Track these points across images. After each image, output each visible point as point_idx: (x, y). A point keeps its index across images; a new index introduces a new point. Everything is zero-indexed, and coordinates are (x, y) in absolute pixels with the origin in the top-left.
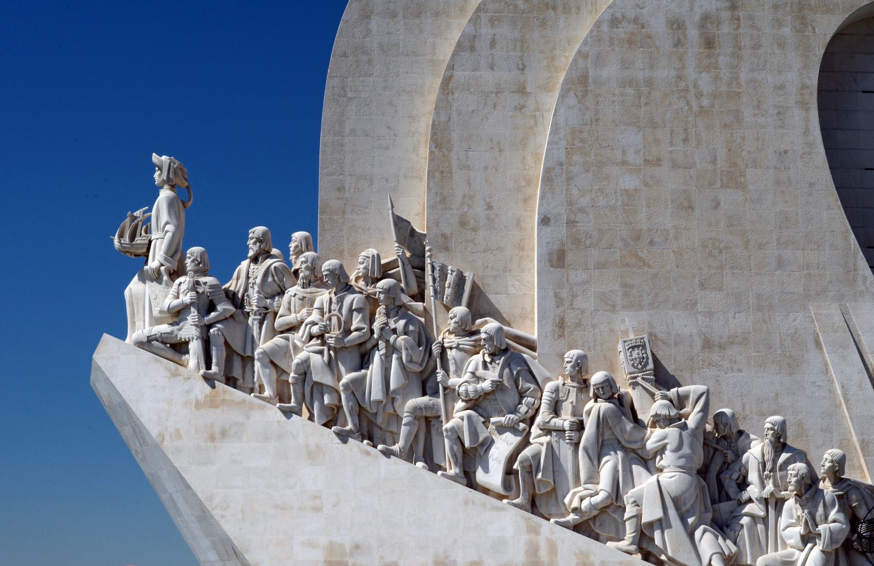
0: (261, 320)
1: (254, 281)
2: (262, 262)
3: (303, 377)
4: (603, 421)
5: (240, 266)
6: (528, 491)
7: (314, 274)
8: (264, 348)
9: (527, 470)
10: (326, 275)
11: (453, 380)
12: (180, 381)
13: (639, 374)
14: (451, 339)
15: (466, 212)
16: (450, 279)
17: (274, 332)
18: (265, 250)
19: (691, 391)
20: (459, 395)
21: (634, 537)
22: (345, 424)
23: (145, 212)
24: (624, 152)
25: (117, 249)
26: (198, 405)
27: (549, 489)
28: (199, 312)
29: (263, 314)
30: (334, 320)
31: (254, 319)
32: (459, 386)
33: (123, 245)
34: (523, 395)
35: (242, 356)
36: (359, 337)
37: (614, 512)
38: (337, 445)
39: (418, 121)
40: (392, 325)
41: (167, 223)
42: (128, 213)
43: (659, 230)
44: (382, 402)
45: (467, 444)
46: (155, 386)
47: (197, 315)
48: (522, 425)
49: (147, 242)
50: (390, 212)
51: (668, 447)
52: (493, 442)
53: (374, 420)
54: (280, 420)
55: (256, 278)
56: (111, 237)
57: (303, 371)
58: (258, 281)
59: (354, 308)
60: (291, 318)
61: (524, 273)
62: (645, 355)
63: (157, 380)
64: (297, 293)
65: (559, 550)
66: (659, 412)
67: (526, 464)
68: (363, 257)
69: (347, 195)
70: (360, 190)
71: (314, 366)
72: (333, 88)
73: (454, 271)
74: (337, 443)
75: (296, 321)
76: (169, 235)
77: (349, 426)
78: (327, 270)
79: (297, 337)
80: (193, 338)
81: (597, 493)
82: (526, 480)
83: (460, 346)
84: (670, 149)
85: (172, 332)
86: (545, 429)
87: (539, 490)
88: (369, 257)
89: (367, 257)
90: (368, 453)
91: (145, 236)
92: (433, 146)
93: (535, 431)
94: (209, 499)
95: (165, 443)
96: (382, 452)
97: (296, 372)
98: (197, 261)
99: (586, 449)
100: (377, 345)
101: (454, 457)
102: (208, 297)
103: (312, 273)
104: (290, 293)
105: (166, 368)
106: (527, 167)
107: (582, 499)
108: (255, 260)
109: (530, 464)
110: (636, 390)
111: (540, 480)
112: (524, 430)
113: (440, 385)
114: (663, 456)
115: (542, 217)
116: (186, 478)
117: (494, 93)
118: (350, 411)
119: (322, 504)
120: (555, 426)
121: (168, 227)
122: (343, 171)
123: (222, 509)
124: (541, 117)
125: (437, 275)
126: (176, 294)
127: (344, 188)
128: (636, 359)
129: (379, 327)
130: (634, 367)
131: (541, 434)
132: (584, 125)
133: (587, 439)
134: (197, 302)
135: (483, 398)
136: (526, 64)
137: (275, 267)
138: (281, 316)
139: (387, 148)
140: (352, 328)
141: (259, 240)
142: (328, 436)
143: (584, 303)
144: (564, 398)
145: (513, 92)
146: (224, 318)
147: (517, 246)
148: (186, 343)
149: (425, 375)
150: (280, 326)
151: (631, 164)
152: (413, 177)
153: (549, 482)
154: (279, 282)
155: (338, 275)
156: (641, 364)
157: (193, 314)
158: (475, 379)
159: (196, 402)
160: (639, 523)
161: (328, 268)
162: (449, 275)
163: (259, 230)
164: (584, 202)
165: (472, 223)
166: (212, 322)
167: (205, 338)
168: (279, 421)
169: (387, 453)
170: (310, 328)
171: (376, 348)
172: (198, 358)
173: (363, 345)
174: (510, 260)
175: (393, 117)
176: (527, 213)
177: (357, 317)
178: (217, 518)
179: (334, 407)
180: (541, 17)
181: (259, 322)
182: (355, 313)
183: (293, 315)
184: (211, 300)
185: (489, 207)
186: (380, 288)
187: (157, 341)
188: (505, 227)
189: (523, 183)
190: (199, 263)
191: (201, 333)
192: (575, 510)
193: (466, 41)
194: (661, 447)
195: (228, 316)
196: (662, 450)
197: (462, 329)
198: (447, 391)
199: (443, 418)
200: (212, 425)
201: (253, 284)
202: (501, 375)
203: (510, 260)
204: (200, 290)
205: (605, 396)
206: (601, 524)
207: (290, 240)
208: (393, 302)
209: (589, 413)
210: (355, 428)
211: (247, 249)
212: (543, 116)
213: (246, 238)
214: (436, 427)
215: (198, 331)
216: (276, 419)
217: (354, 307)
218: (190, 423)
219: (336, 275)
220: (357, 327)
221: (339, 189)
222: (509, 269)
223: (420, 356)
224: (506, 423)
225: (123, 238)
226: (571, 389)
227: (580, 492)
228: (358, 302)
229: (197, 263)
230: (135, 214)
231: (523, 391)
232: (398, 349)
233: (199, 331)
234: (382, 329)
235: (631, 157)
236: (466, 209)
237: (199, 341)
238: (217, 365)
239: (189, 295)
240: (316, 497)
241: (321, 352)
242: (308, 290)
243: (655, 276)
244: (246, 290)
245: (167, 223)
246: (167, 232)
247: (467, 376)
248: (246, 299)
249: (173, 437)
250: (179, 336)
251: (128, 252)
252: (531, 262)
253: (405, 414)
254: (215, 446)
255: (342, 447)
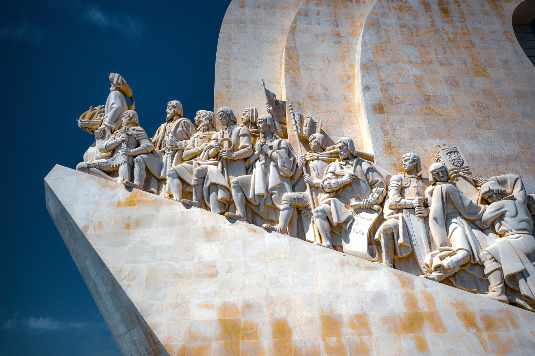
0: (173, 155)
1: (169, 131)
2: (175, 121)
3: (202, 180)
4: (446, 198)
5: (161, 127)
6: (391, 256)
7: (211, 124)
8: (175, 168)
9: (389, 237)
10: (220, 116)
11: (316, 181)
12: (108, 190)
13: (461, 170)
14: (312, 154)
15: (312, 91)
16: (306, 122)
17: (183, 161)
18: (178, 114)
19: (507, 177)
20: (323, 188)
21: (502, 287)
22: (235, 210)
23: (101, 108)
24: (409, 57)
25: (80, 127)
26: (119, 204)
27: (409, 254)
28: (128, 146)
29: (174, 151)
30: (226, 144)
31: (167, 154)
32: (323, 182)
33: (83, 122)
34: (373, 186)
35: (158, 179)
36: (245, 152)
37: (471, 269)
38: (229, 227)
39: (275, 55)
40: (269, 144)
41: (113, 104)
42: (90, 107)
43: (441, 96)
44: (263, 196)
45: (335, 220)
46: (88, 194)
47: (126, 147)
48: (376, 207)
49: (100, 121)
50: (263, 86)
51: (507, 214)
52: (354, 220)
53: (257, 212)
54: (183, 211)
55: (170, 130)
56: (77, 120)
57: (202, 176)
58: (172, 129)
59: (240, 134)
60: (194, 150)
61: (353, 125)
62: (460, 158)
63: (90, 190)
64: (199, 135)
65: (436, 301)
66: (492, 188)
67: (389, 232)
68: (246, 111)
69: (232, 90)
70: (241, 87)
71: (211, 172)
72: (224, 37)
73: (309, 118)
74: (228, 225)
75: (198, 151)
76: (114, 109)
77: (238, 213)
78: (221, 111)
79: (199, 160)
80: (122, 164)
81: (454, 253)
82: (389, 246)
83: (319, 157)
84: (436, 56)
85: (107, 163)
86: (395, 209)
87: (401, 255)
88: (250, 110)
89: (248, 110)
90: (255, 231)
91: (99, 118)
92: (287, 59)
93: (387, 211)
94: (119, 273)
95: (89, 232)
96: (265, 228)
97: (197, 176)
98: (130, 117)
99: (435, 219)
100: (259, 158)
101: (325, 232)
102: (136, 138)
103: (209, 122)
104: (194, 136)
105: (98, 182)
106: (346, 71)
107: (442, 258)
108: (171, 120)
109: (392, 232)
110: (459, 181)
111: (401, 245)
112: (379, 210)
113: (307, 184)
114: (502, 222)
115: (365, 87)
116: (101, 258)
117: (322, 35)
118: (239, 202)
119: (217, 271)
120: (405, 204)
121: (114, 106)
122: (229, 78)
123: (129, 280)
124: (351, 48)
125: (297, 119)
126: (113, 139)
127: (230, 86)
128: (455, 160)
129: (259, 144)
130: (455, 165)
131: (393, 212)
132: (382, 43)
133: (435, 212)
134: (127, 140)
135: (342, 191)
136: (338, 23)
137: (184, 122)
138: (187, 149)
139: (257, 67)
140: (239, 147)
141: (173, 107)
142: (222, 220)
143: (402, 134)
144: (408, 185)
145: (333, 35)
146: (147, 152)
147: (346, 110)
148: (118, 167)
149: (294, 181)
150: (187, 155)
151: (414, 62)
152: (273, 82)
153: (409, 247)
154: (187, 131)
155: (229, 115)
156: (460, 164)
157: (123, 147)
158: (334, 176)
159: (118, 202)
160: (503, 276)
161: (222, 110)
162: (305, 120)
163: (174, 102)
164: (390, 80)
165: (316, 97)
166: (137, 153)
167: (131, 164)
168: (182, 212)
169: (269, 230)
170: (208, 152)
171: (258, 161)
172: (124, 176)
173: (247, 160)
174: (343, 118)
175: (260, 53)
176: (350, 94)
177: (243, 140)
178: (124, 288)
179: (226, 203)
180: (344, 4)
181: (172, 156)
182: (241, 138)
183: (196, 148)
184: (137, 140)
185: (326, 89)
186: (259, 120)
187: (96, 168)
188: (337, 100)
189: (345, 78)
190: (131, 119)
191: (128, 159)
192: (439, 268)
193: (303, 12)
194: (499, 215)
195: (149, 151)
196: (501, 217)
197: (320, 147)
198: (313, 189)
199: (312, 206)
200: (129, 217)
201: (169, 133)
202: (354, 171)
203: (343, 118)
204: (130, 133)
205: (444, 179)
206: (461, 280)
207: (195, 115)
208: (269, 129)
209: (431, 193)
210: (243, 214)
211: (166, 114)
212: (352, 47)
213: (166, 107)
214: (306, 214)
215: (125, 158)
216: (180, 211)
217: (240, 134)
218: (111, 217)
219: (228, 114)
220: (243, 145)
221: (227, 87)
222: (343, 123)
223: (291, 164)
224: (364, 205)
225: (84, 118)
226: (412, 179)
227: (437, 254)
228: (243, 131)
229: (129, 118)
230: (95, 108)
231: (372, 184)
232: (274, 160)
233: (127, 157)
234: (262, 146)
235: (413, 59)
236: (311, 90)
237: (126, 164)
238: (140, 180)
239: (121, 137)
240: (211, 266)
241: (216, 165)
242: (207, 133)
243: (445, 121)
244: (163, 138)
245: (113, 104)
246: (113, 108)
247: (329, 175)
248: (163, 143)
249: (96, 228)
250: (112, 164)
251: (87, 128)
252: (357, 119)
253: (283, 203)
254: (129, 232)
255: (233, 227)
